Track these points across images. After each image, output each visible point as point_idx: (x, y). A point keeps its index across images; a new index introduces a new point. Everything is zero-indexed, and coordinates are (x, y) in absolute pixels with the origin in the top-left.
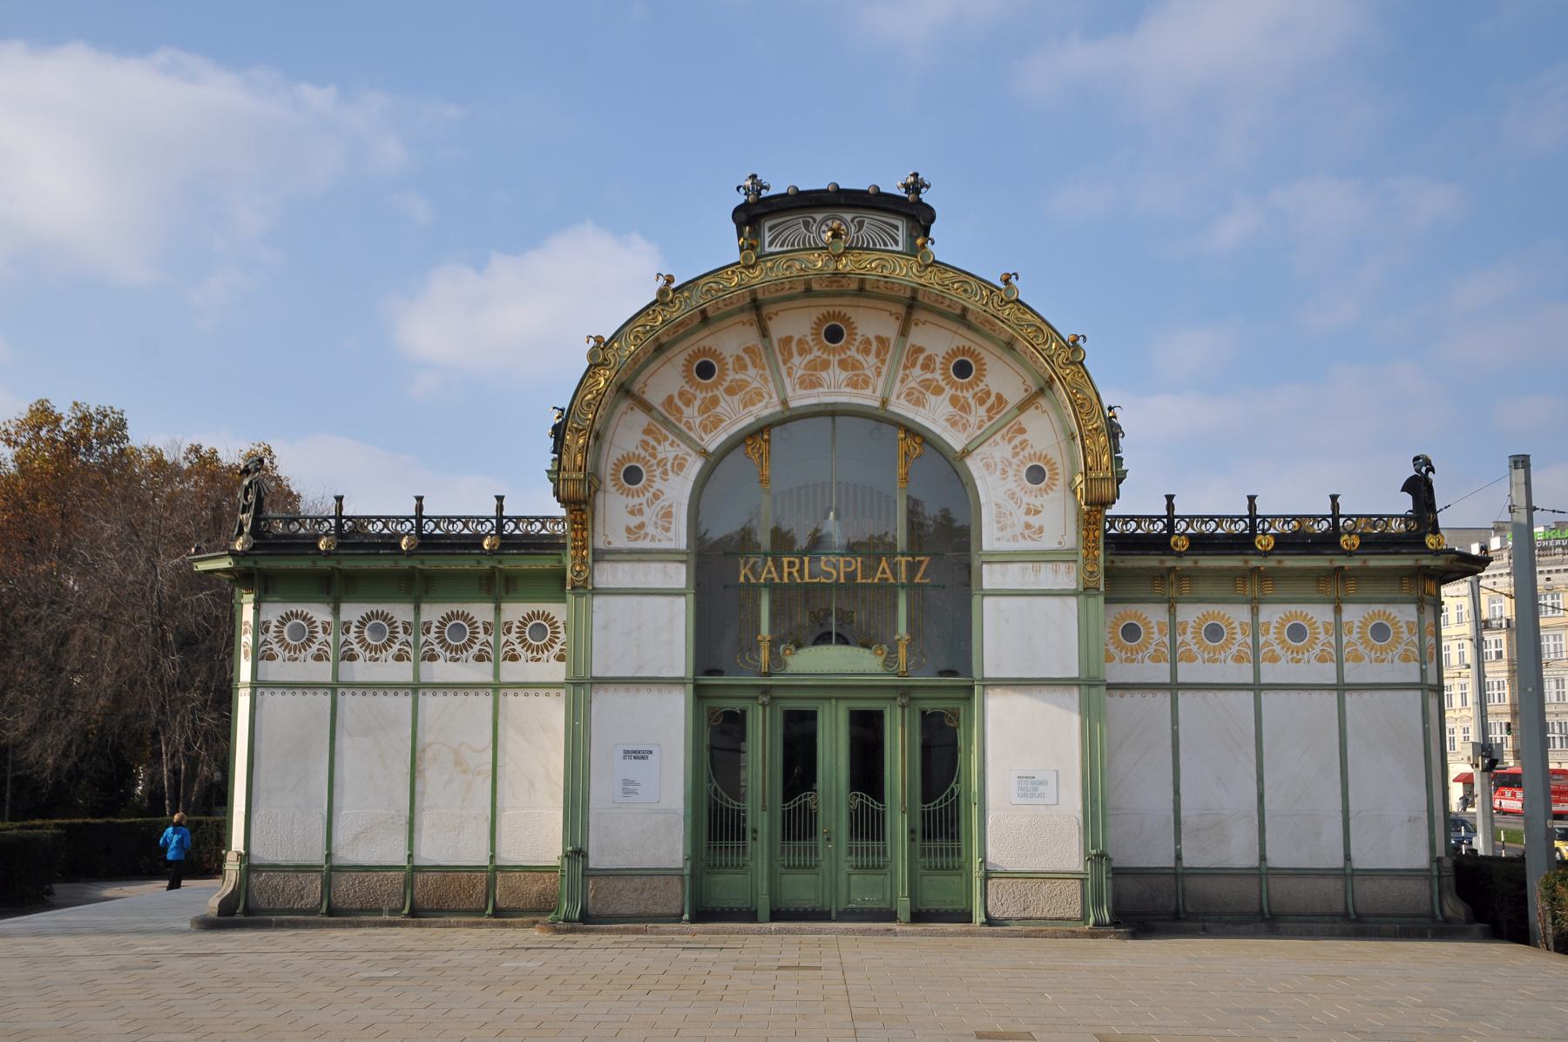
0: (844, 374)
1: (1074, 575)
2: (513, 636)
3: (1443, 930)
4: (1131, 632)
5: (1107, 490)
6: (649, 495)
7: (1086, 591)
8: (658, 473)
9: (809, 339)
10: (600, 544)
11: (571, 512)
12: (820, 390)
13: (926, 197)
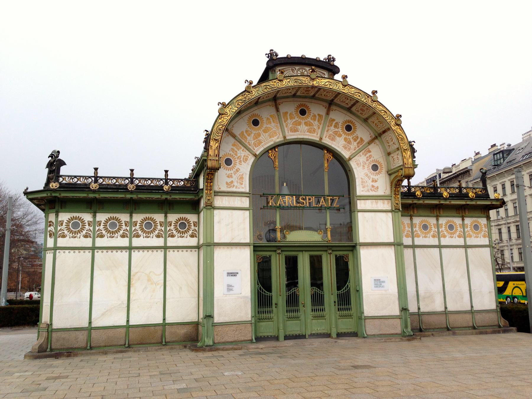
0: (307, 127)
1: (390, 204)
3: (497, 330)
5: (411, 172)
6: (234, 170)
8: (238, 161)
9: (294, 113)
10: (216, 188)
12: (298, 133)
13: (336, 63)
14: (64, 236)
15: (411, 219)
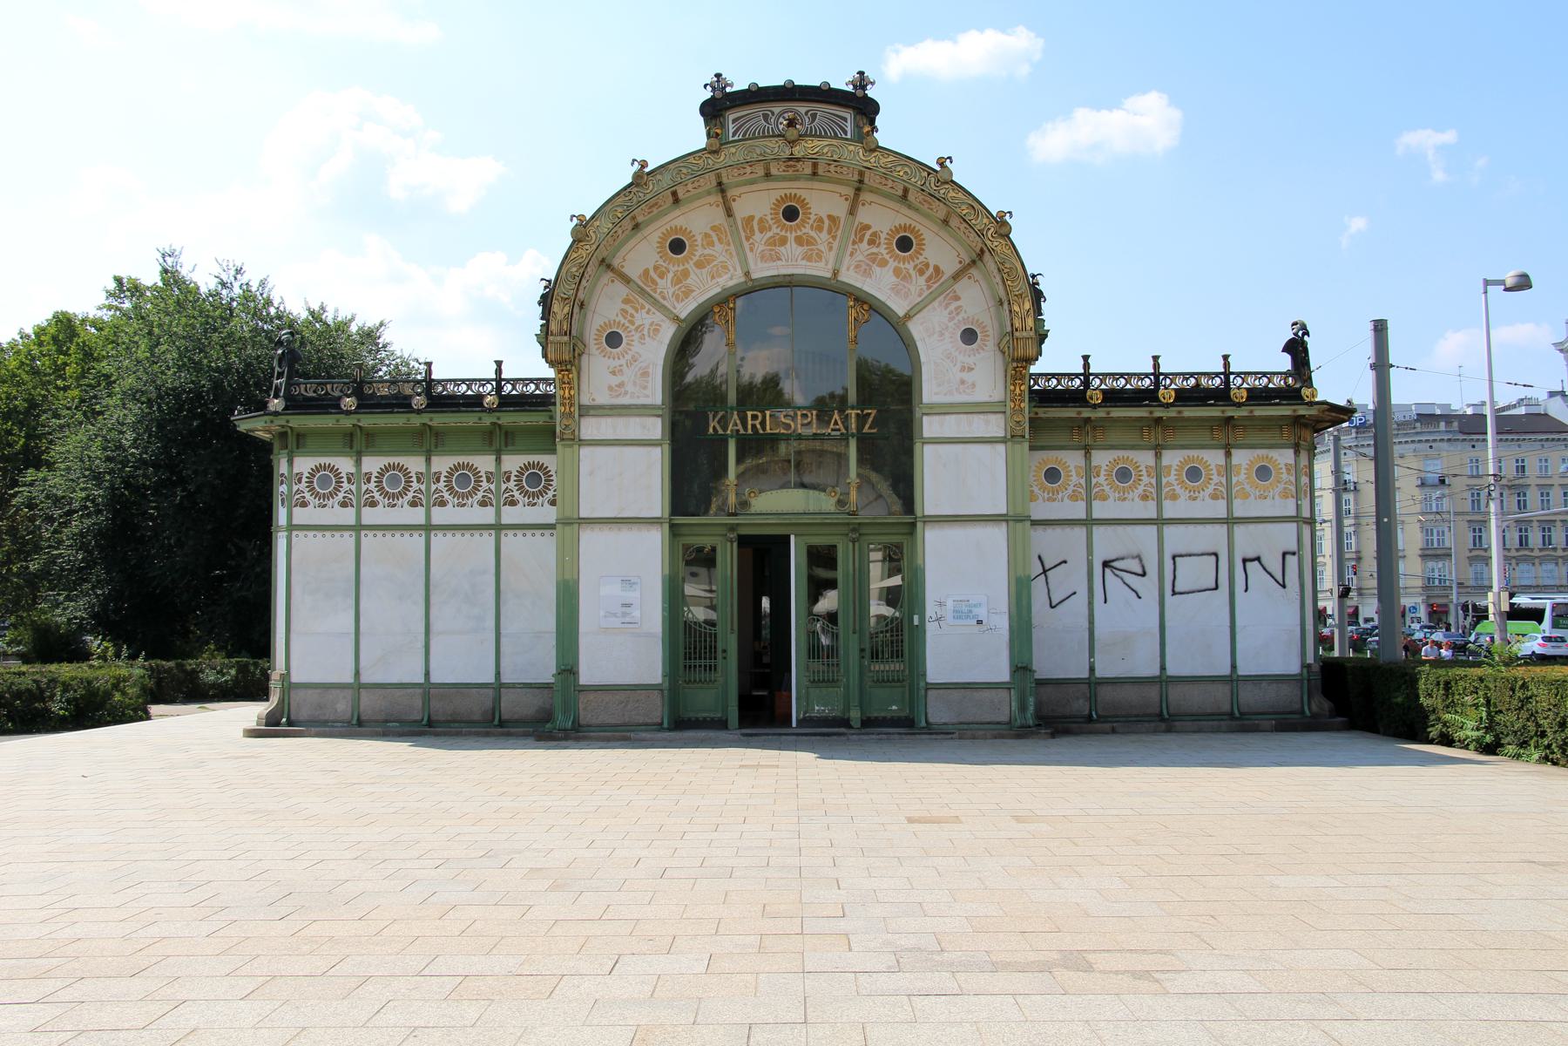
0: (800, 249)
2: (512, 484)
4: (1052, 475)
7: (1012, 438)
8: (637, 336)
10: (585, 400)
11: (559, 372)
13: (871, 92)
14: (304, 504)
15: (1088, 456)
